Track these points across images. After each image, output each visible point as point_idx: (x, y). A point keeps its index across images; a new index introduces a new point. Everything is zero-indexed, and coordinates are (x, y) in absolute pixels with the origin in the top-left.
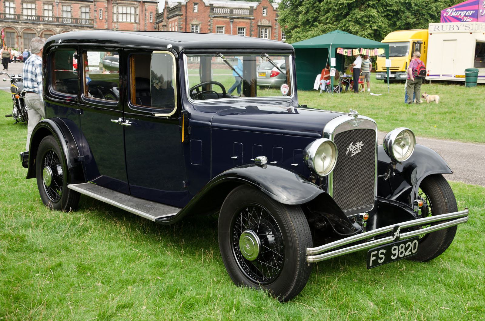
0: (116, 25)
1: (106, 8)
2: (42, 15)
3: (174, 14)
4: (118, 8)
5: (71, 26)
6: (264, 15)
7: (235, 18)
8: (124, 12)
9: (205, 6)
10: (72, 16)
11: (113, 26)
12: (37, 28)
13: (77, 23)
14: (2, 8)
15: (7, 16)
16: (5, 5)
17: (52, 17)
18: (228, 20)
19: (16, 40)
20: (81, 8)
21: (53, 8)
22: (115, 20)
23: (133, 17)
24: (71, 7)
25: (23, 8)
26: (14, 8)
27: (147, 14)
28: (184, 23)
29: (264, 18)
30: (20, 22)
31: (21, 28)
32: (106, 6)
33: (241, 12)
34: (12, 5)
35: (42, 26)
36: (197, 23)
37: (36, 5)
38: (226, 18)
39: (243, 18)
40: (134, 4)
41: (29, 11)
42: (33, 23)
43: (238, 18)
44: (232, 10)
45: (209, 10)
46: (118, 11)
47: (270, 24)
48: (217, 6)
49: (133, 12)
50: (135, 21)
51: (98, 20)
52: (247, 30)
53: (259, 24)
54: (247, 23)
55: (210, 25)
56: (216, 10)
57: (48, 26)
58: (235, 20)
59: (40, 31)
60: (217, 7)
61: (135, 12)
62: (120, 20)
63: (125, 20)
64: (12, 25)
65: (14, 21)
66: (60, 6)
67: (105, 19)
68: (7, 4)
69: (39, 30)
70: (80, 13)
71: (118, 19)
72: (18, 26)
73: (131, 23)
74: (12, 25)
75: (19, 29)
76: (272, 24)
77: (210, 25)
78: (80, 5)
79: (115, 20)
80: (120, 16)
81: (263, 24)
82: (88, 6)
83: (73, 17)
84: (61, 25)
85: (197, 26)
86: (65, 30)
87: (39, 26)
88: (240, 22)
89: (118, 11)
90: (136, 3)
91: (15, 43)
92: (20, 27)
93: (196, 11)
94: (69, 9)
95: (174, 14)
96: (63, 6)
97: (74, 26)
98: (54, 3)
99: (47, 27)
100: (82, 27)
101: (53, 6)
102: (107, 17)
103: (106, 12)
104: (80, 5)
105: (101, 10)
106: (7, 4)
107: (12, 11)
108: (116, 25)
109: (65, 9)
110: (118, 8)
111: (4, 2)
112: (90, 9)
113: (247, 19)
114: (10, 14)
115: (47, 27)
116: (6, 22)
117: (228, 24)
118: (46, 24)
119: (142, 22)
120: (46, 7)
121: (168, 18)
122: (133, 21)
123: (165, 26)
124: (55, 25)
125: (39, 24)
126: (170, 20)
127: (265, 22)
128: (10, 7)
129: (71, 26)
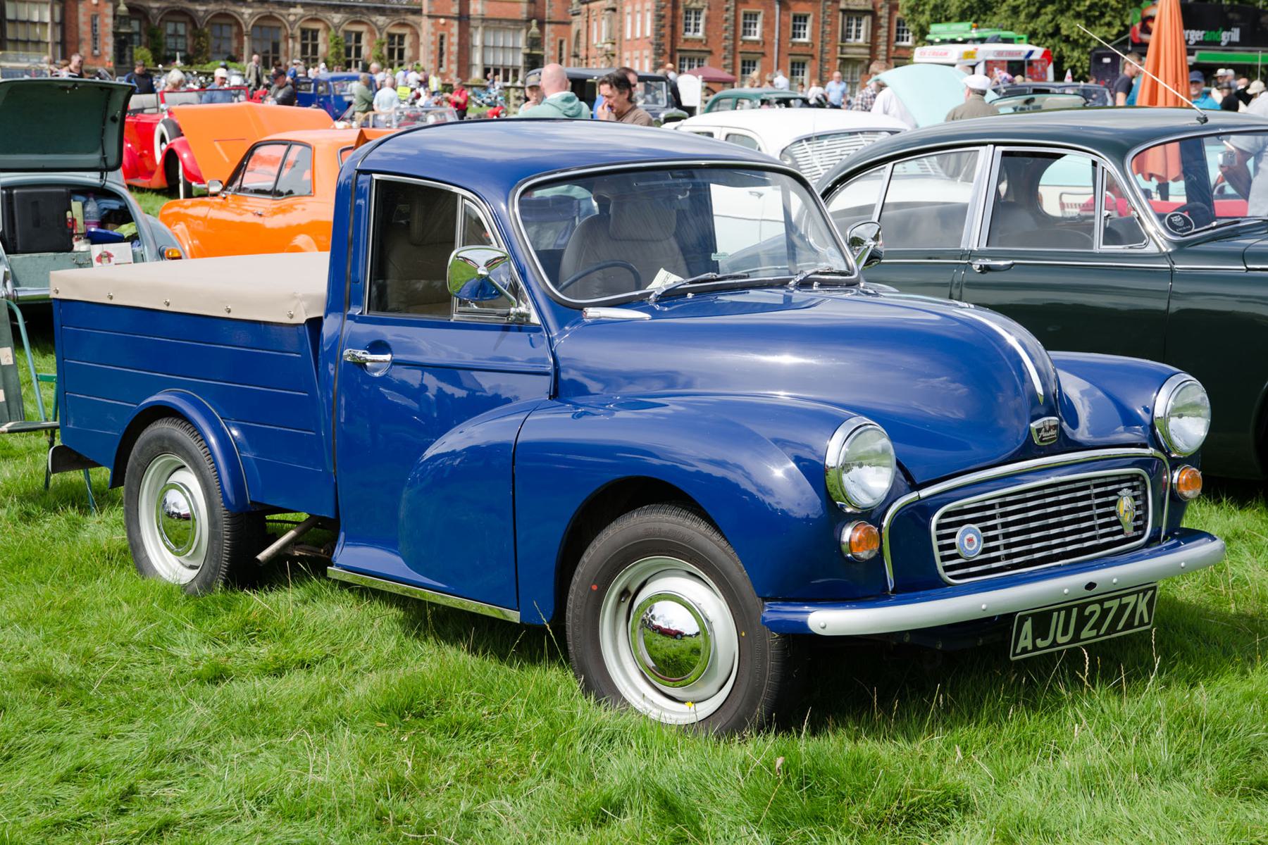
28: (669, 5)
31: (250, 15)
36: (700, 5)
47: (870, 7)
52: (814, 20)
59: (295, 21)
69: (292, 18)
72: (244, 10)
75: (246, 16)
76: (874, 6)
77: (727, 10)
81: (852, 7)
86: (352, 17)
87: (292, 10)
92: (250, 11)
99: (312, 13)
123: (614, 10)
125: (294, 5)
129: (367, 8)
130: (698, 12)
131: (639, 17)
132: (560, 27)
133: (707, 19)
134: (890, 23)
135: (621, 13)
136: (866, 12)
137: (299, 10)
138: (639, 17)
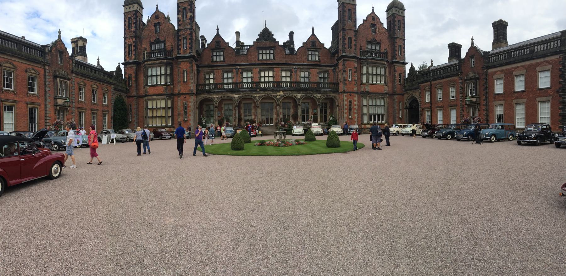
0: (366, 88)
1: (356, 68)
5: (313, 91)
11: (363, 88)
12: (277, 96)
13: (320, 88)
16: (242, 75)
19: (253, 111)
21: (291, 75)
22: (365, 82)
24: (309, 73)
31: (259, 97)
32: (356, 65)
34: (250, 74)
35: (282, 93)
40: (384, 64)
50: (385, 83)
51: (347, 82)
61: (385, 72)
63: (375, 82)
64: (250, 94)
65: (252, 90)
66: (298, 72)
67: (355, 80)
68: (245, 75)
69: (278, 97)
73: (382, 85)
74: (250, 94)
78: (318, 71)
79: (365, 82)
84: (302, 91)
87: (278, 94)
89: (367, 72)
91: (252, 114)
96: (301, 71)
97: (316, 91)
98: (293, 69)
100: (324, 91)
102: (356, 79)
103: (355, 72)
104: (318, 71)
105: (350, 70)
108: (366, 88)
110: (367, 69)
111: (242, 73)
112: (328, 74)
132: (399, 96)
137: (282, 93)
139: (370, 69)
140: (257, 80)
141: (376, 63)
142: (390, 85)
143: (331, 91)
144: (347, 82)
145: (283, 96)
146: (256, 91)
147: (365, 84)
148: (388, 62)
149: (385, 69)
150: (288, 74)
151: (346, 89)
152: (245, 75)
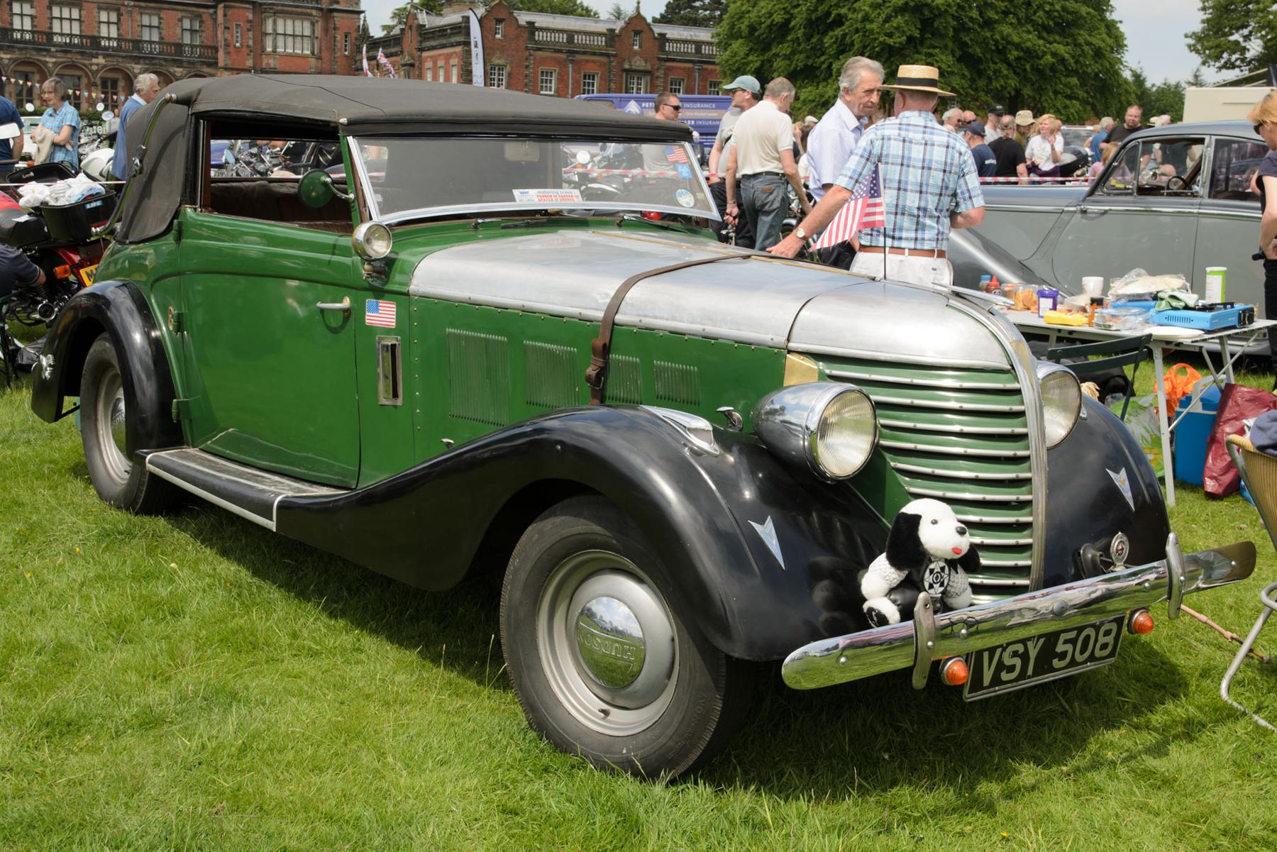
1: (250, 22)
2: (96, 34)
3: (444, 41)
4: (275, 22)
6: (636, 48)
7: (577, 52)
8: (289, 31)
9: (519, 26)
10: (161, 38)
11: (265, 61)
14: (7, 17)
15: (57, 39)
16: (11, 9)
17: (158, 43)
18: (564, 56)
20: (181, 20)
21: (119, 19)
22: (269, 49)
23: (307, 42)
24: (160, 18)
25: (53, 18)
26: (32, 17)
27: (339, 38)
29: (636, 53)
30: (53, 49)
32: (251, 17)
33: (682, 48)
34: (27, 9)
35: (101, 60)
36: (501, 62)
37: (83, 12)
38: (560, 51)
39: (594, 54)
40: (311, 15)
41: (66, 24)
42: (82, 54)
43: (584, 53)
44: (571, 34)
45: (526, 35)
46: (275, 30)
47: (649, 68)
48: (544, 25)
49: (307, 32)
50: (313, 53)
53: (627, 66)
54: (602, 64)
55: (527, 67)
56: (539, 36)
57: (115, 59)
58: (579, 57)
59: (98, 71)
60: (541, 29)
61: (313, 32)
62: (280, 50)
63: (290, 51)
69: (94, 68)
70: (179, 31)
71: (275, 47)
73: (304, 57)
74: (35, 56)
77: (527, 67)
78: (180, 15)
79: (269, 49)
80: (280, 40)
82: (199, 16)
83: (166, 40)
85: (501, 68)
87: (94, 61)
88: (587, 61)
89: (275, 30)
90: (314, 12)
93: (498, 36)
94: (155, 22)
95: (444, 41)
100: (189, 62)
101: (119, 15)
102: (251, 43)
106: (56, 12)
107: (28, 25)
109: (146, 20)
110: (275, 22)
111: (10, 4)
112: (201, 22)
113: (601, 54)
114: (109, 39)
115: (113, 62)
116: (20, 49)
117: (562, 64)
118: (110, 56)
119: (325, 55)
120: (104, 16)
121: (421, 50)
122: (307, 52)
123: (412, 65)
124: (131, 57)
126: (425, 54)
127: (639, 64)
128: (61, 19)
129: (166, 60)
130: (501, 68)
131: (441, 73)
133: (510, 75)
134: (665, 82)
135: (420, 69)
136: (645, 72)
137: (101, 60)
138: (441, 73)
139: (280, 22)
140: (43, 27)
141: (291, 13)
142: (325, 55)
143: (203, 63)
144: (231, 49)
145: (104, 66)
146: (48, 51)
147: (268, 54)
148: (321, 10)
149: (313, 24)
150: (114, 17)
151: (229, 62)
152: (16, 8)
